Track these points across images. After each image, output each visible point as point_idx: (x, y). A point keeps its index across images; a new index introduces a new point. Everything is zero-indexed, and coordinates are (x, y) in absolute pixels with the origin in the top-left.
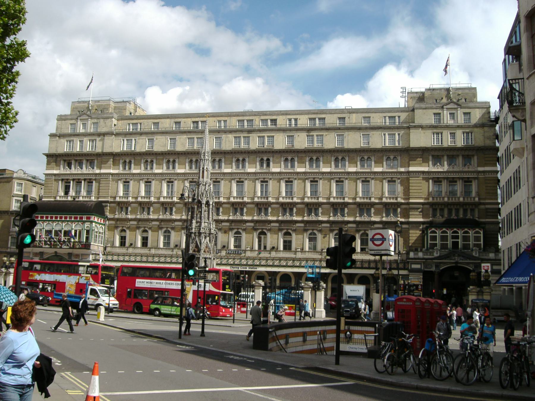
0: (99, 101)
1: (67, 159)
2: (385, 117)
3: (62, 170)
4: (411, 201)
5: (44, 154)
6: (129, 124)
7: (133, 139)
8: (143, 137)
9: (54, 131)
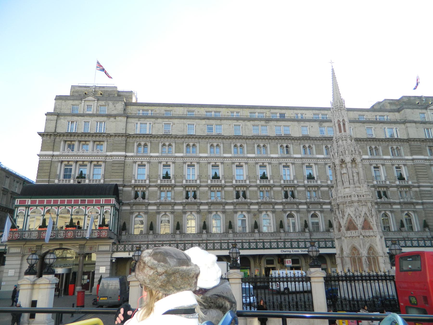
0: (103, 87)
1: (70, 138)
2: (376, 116)
3: (62, 151)
4: (420, 184)
5: (40, 134)
6: (139, 110)
7: (148, 123)
8: (160, 120)
9: (52, 111)
